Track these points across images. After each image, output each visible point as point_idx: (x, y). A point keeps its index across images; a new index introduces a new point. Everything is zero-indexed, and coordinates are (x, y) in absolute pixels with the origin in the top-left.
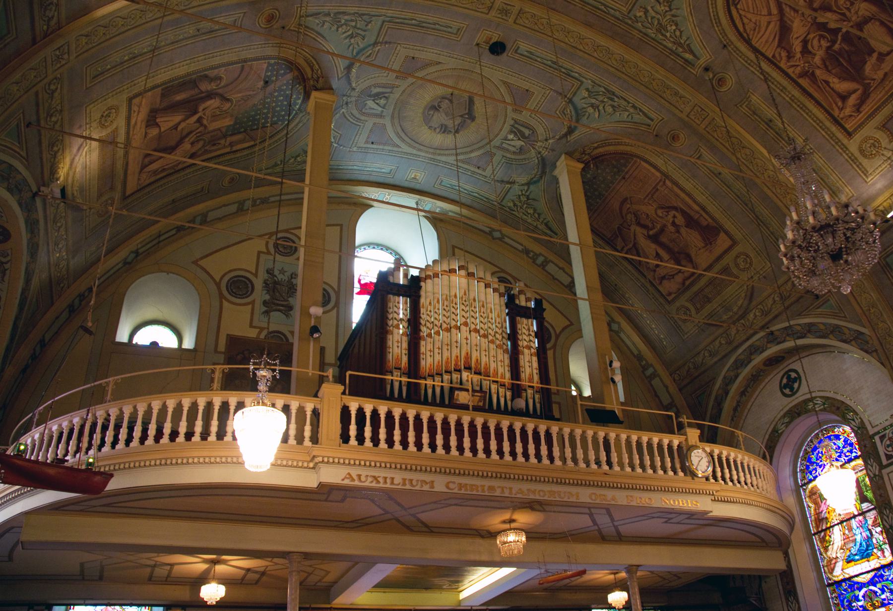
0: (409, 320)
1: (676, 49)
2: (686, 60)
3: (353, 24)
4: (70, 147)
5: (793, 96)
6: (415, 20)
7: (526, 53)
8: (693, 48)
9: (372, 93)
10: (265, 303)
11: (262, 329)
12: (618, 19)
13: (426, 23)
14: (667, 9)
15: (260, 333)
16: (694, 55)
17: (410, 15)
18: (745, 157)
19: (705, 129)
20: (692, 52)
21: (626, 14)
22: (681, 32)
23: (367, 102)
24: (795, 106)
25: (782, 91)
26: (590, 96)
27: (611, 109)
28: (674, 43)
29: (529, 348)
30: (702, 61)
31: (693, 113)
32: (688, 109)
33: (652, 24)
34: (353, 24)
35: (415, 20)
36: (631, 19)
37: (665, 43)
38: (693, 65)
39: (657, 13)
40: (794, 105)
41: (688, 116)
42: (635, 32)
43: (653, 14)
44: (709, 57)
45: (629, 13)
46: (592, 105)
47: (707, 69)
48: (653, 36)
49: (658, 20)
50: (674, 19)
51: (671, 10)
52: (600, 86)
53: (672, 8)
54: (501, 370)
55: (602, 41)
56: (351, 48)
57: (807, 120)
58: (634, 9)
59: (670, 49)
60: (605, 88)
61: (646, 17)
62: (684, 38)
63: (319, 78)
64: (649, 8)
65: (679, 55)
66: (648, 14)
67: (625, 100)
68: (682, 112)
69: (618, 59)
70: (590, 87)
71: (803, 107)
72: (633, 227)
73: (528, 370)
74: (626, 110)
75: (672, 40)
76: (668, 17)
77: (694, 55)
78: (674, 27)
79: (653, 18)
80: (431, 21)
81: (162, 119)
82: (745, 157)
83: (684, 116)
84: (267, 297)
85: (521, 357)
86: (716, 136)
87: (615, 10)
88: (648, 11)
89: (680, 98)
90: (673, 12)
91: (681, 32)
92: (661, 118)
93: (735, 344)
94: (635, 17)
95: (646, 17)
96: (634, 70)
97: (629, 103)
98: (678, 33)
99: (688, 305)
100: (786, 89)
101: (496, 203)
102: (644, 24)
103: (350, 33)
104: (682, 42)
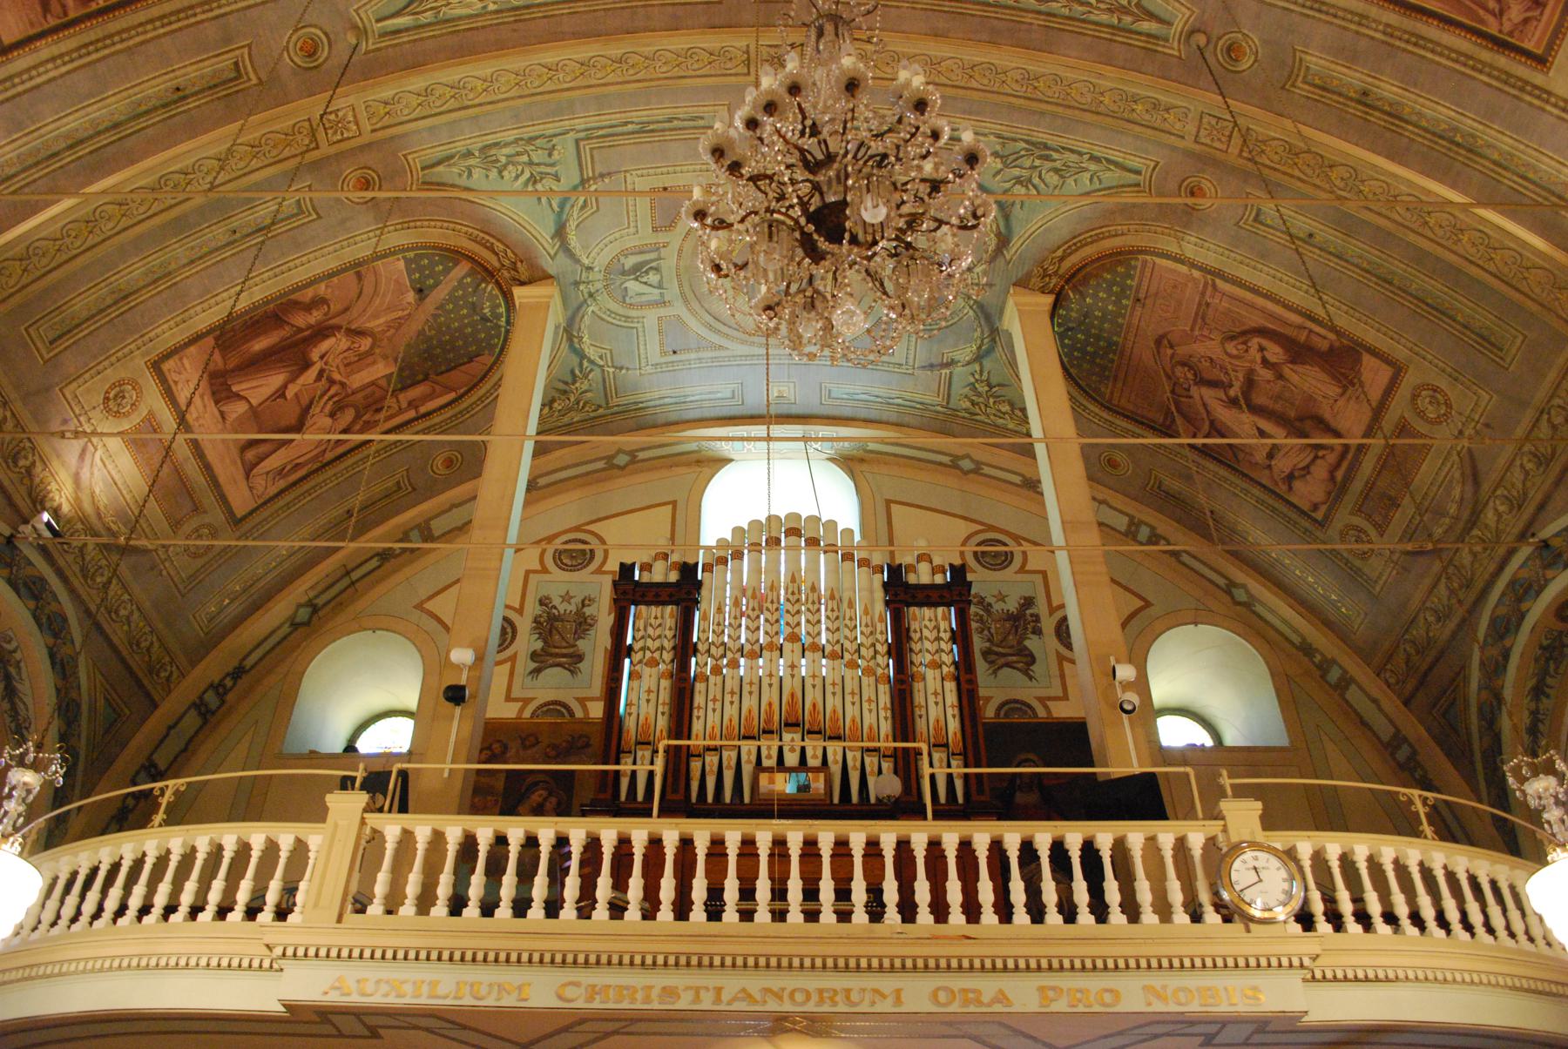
0: (674, 648)
1: (1120, 20)
3: (525, 158)
4: (58, 456)
5: (1388, 25)
6: (632, 123)
9: (626, 268)
10: (534, 656)
11: (526, 701)
13: (653, 123)
15: (521, 710)
16: (1160, 20)
17: (617, 118)
18: (1342, 185)
19: (1240, 155)
20: (1152, 16)
23: (627, 284)
24: (1403, 45)
25: (1360, 24)
26: (1006, 166)
27: (1056, 178)
29: (937, 665)
30: (1178, 25)
31: (1203, 133)
32: (1191, 128)
34: (525, 158)
35: (632, 123)
37: (1092, 17)
40: (1398, 43)
41: (1196, 142)
42: (1029, 18)
44: (1188, 13)
46: (1019, 181)
52: (1015, 140)
54: (869, 719)
56: (544, 200)
57: (1439, 64)
59: (1108, 26)
60: (1027, 142)
63: (515, 263)
65: (1131, 32)
67: (1072, 151)
68: (1183, 137)
69: (1019, 77)
70: (998, 148)
71: (1419, 40)
72: (1194, 391)
73: (934, 712)
74: (1086, 170)
77: (1160, 20)
80: (660, 118)
81: (244, 386)
82: (1342, 185)
83: (1188, 144)
84: (539, 645)
85: (918, 686)
86: (1268, 162)
92: (1152, 164)
93: (1479, 585)
97: (1080, 154)
99: (1357, 521)
100: (1367, 17)
101: (939, 408)
103: (527, 175)
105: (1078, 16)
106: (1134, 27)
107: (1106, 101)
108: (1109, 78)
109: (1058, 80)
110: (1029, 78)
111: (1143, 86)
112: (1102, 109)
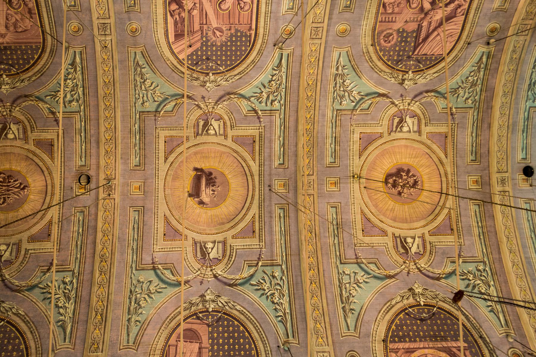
1: (482, 68)
2: (488, 58)
6: (531, 235)
7: (524, 152)
8: (478, 59)
12: (478, 111)
13: (530, 227)
14: (460, 88)
17: (530, 241)
21: (473, 109)
22: (471, 72)
28: (479, 72)
33: (473, 91)
35: (531, 235)
36: (475, 105)
37: (482, 77)
38: (489, 52)
39: (465, 92)
42: (483, 97)
43: (467, 94)
45: (472, 108)
47: (488, 44)
48: (480, 86)
49: (469, 89)
50: (464, 82)
51: (460, 86)
53: (458, 86)
55: (497, 113)
58: (468, 106)
61: (470, 97)
62: (474, 68)
64: (464, 98)
65: (486, 64)
66: (468, 97)
67: (531, 75)
69: (504, 98)
75: (478, 75)
76: (465, 85)
78: (470, 78)
79: (469, 93)
80: (528, 224)
87: (474, 116)
88: (466, 98)
89: (515, 47)
90: (460, 84)
91: (471, 72)
94: (472, 103)
95: (470, 97)
96: (508, 85)
97: (532, 72)
98: (472, 74)
102: (475, 96)
104: (476, 68)
105: (481, 82)
106: (485, 63)
107: (512, 68)
108: (503, 68)
109: (505, 85)
110: (505, 94)
111: (506, 57)
112: (515, 69)
